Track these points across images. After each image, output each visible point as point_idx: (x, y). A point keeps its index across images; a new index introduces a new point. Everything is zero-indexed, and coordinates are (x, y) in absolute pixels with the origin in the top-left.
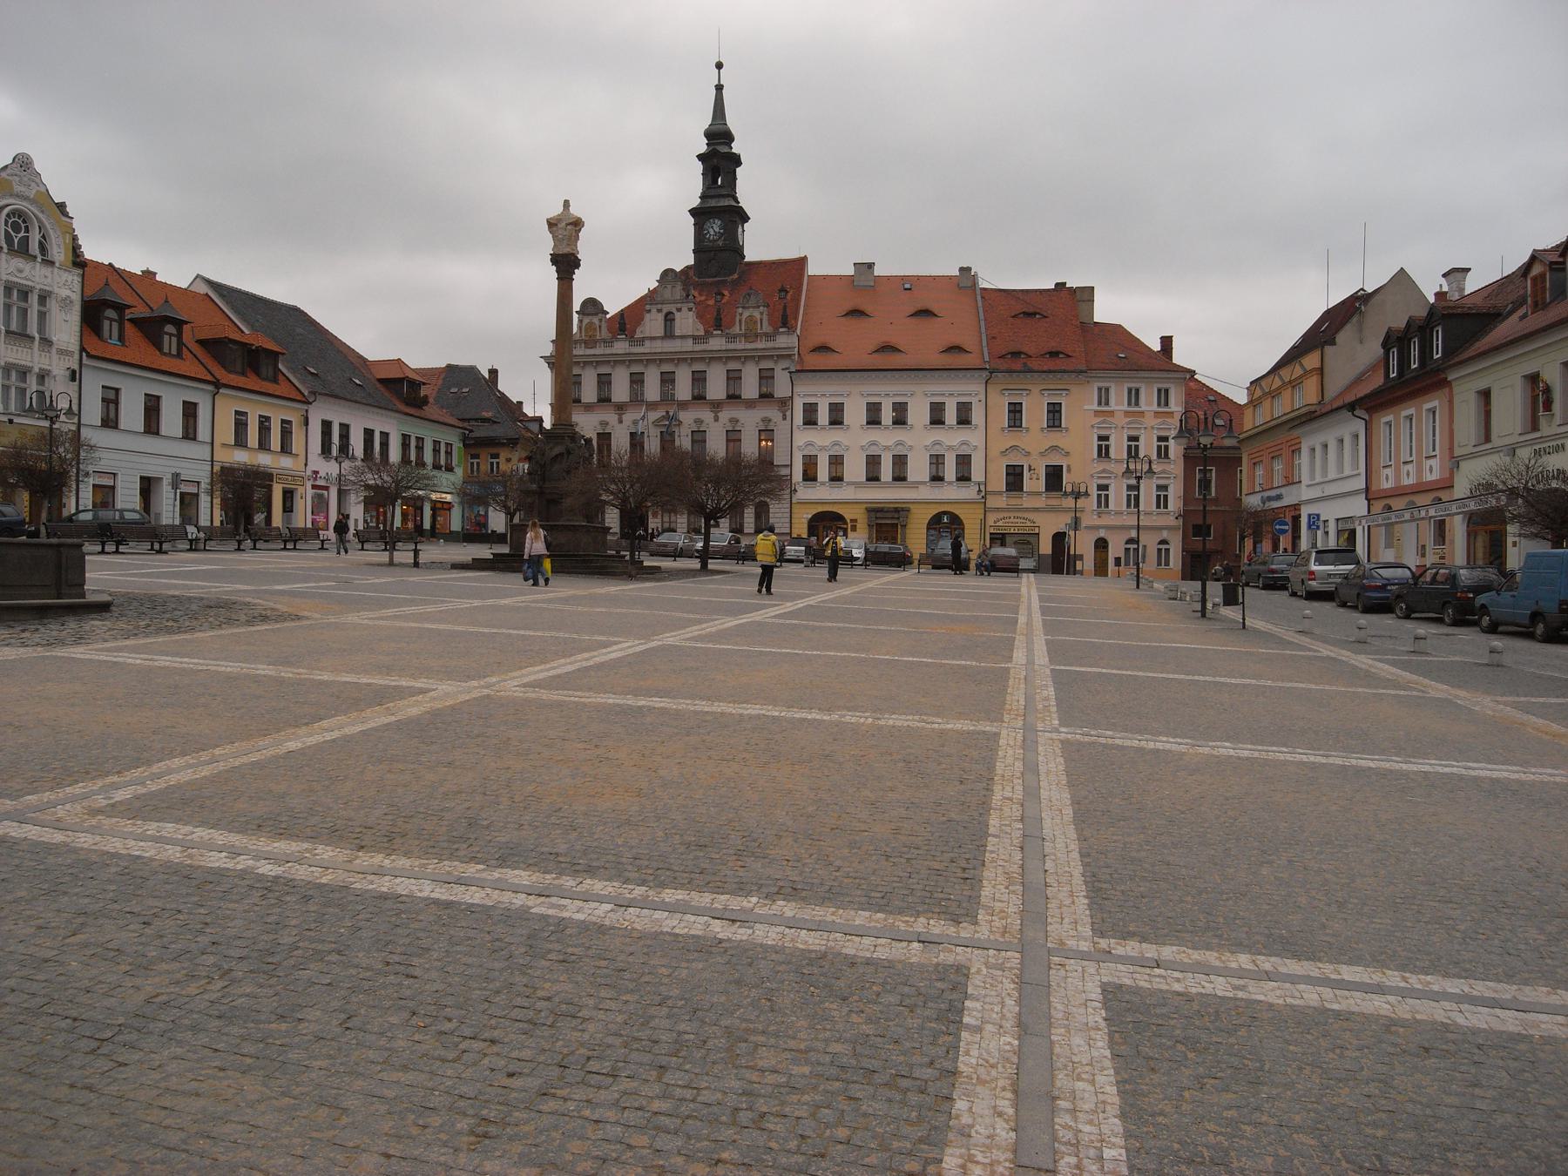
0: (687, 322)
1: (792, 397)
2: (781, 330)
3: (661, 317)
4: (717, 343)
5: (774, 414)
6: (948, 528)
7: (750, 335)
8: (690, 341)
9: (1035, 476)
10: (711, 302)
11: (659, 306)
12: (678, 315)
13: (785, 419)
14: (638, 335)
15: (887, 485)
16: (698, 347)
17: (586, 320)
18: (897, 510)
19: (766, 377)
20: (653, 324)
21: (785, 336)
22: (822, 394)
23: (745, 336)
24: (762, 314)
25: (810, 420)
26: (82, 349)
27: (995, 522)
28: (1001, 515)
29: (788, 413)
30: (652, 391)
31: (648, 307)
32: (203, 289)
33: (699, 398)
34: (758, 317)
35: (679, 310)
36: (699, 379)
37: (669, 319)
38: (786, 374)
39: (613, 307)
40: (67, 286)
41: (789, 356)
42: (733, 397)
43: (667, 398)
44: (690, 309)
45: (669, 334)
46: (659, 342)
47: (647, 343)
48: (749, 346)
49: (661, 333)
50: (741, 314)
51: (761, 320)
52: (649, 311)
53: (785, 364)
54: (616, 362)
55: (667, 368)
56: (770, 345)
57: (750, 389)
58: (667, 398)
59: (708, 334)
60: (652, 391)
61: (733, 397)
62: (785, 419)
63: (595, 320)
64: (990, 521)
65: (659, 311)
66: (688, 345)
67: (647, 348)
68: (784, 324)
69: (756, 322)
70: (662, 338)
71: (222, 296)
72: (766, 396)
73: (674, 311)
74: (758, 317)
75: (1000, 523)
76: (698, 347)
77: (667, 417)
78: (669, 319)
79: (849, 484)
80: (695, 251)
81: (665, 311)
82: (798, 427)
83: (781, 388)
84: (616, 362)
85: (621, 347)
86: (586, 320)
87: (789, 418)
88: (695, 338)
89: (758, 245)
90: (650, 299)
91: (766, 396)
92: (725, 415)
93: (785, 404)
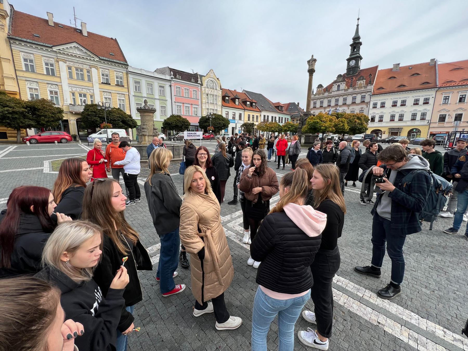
0: (343, 86)
3: (336, 86)
4: (351, 90)
5: (364, 106)
10: (350, 81)
12: (341, 85)
13: (367, 107)
14: (331, 91)
16: (346, 92)
17: (318, 90)
19: (363, 97)
20: (335, 88)
22: (379, 100)
23: (358, 88)
24: (364, 81)
25: (375, 107)
26: (222, 105)
30: (333, 104)
32: (244, 92)
33: (344, 104)
35: (341, 84)
36: (345, 100)
39: (325, 86)
40: (220, 93)
41: (370, 91)
42: (354, 103)
43: (337, 105)
45: (338, 90)
46: (335, 92)
47: (333, 93)
48: (359, 90)
49: (336, 89)
54: (325, 98)
56: (365, 89)
57: (358, 100)
58: (337, 105)
59: (348, 88)
60: (333, 104)
61: (354, 103)
62: (367, 107)
63: (321, 89)
65: (336, 85)
66: (343, 92)
67: (333, 94)
68: (370, 83)
70: (337, 91)
71: (247, 93)
72: (363, 102)
73: (340, 84)
76: (346, 92)
77: (336, 109)
80: (347, 69)
81: (338, 84)
83: (367, 100)
84: (325, 98)
85: (326, 94)
86: (318, 90)
88: (345, 90)
89: (363, 65)
90: (335, 82)
91: (363, 102)
92: (351, 107)
93: (368, 103)
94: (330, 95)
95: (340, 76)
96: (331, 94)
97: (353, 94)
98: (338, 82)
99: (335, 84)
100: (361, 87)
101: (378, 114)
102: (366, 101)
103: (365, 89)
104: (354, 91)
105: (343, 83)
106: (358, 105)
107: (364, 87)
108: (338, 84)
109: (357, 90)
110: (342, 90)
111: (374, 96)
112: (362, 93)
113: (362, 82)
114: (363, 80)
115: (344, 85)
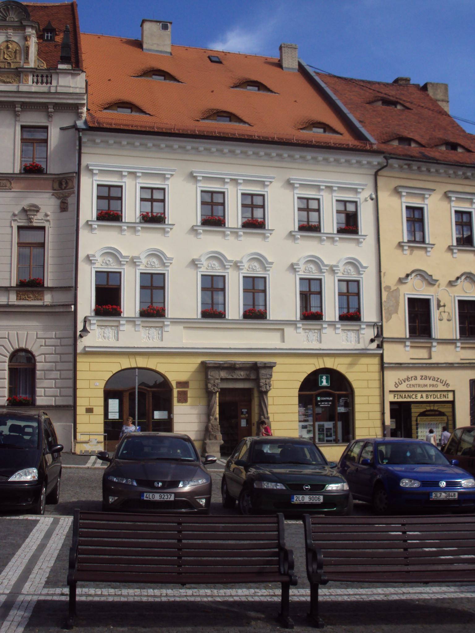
1: (79, 174)
2: (60, 66)
6: (329, 395)
9: (445, 316)
15: (234, 325)
18: (255, 368)
21: (70, 77)
27: (396, 385)
28: (403, 374)
29: (71, 200)
41: (75, 108)
56: (43, 88)
62: (64, 207)
64: (390, 385)
75: (403, 387)
79: (176, 321)
82: (88, 224)
87: (72, 207)
101: (134, 262)
102: (54, 168)
103: (43, 88)
111: (99, 137)
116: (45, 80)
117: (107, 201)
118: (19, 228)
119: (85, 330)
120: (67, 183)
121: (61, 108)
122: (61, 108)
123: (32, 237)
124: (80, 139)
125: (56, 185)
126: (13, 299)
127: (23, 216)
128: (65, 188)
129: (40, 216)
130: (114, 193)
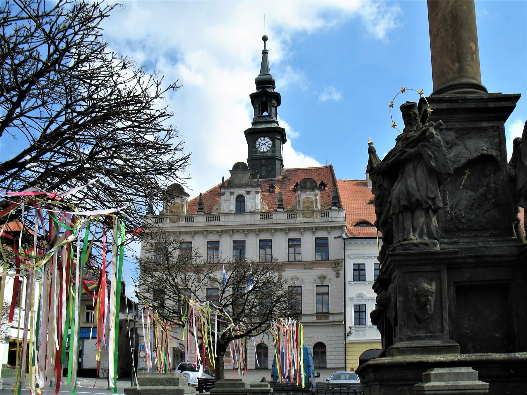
3: (233, 199)
4: (281, 218)
5: (329, 272)
7: (309, 211)
8: (258, 217)
11: (232, 190)
12: (247, 197)
23: (303, 212)
29: (342, 272)
31: (223, 191)
34: (313, 198)
35: (248, 193)
37: (240, 200)
38: (340, 240)
44: (258, 193)
47: (222, 218)
49: (233, 208)
50: (299, 196)
51: (316, 200)
52: (223, 194)
53: (337, 233)
55: (238, 237)
62: (338, 276)
65: (232, 194)
68: (335, 204)
69: (311, 202)
73: (244, 194)
74: (313, 198)
76: (266, 221)
78: (240, 200)
84: (195, 233)
90: (226, 185)
94: (212, 223)
95: (238, 167)
96: (216, 223)
97: (290, 230)
98: (238, 186)
99: (227, 192)
100: (313, 212)
103: (324, 219)
104: (292, 221)
105: (253, 191)
106: (309, 268)
107: (320, 211)
108: (238, 192)
109: (300, 219)
110: (253, 213)
111: (353, 242)
112: (317, 229)
113: (311, 195)
114: (313, 189)
115: (259, 197)
116: (325, 215)
117: (358, 271)
118: (316, 286)
119: (350, 332)
120: (338, 264)
121: (333, 228)
122: (333, 228)
123: (324, 290)
124: (345, 243)
125: (334, 265)
126: (314, 319)
127: (318, 281)
128: (338, 267)
129: (327, 280)
130: (361, 267)
